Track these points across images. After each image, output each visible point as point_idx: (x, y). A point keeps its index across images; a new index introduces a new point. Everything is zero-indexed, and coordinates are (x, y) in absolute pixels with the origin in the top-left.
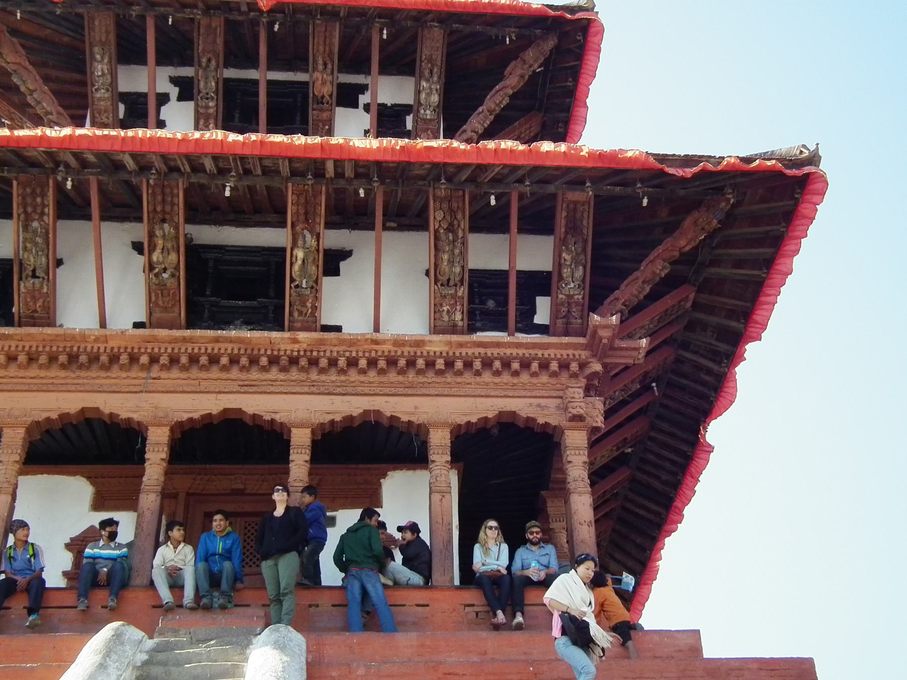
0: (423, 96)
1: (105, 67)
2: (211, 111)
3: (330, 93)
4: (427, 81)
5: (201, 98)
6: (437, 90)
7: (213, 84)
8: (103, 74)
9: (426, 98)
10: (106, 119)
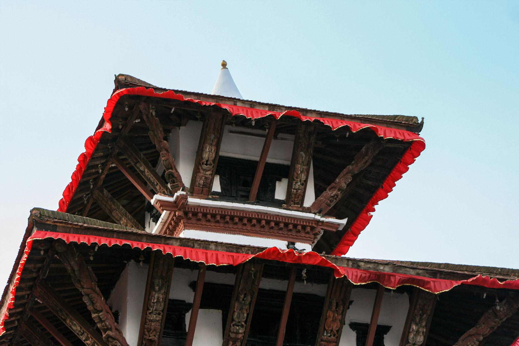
0: (411, 336)
1: (161, 296)
2: (240, 336)
3: (337, 329)
4: (417, 324)
5: (233, 325)
6: (423, 332)
7: (245, 315)
8: (158, 301)
9: (413, 338)
10: (154, 337)
